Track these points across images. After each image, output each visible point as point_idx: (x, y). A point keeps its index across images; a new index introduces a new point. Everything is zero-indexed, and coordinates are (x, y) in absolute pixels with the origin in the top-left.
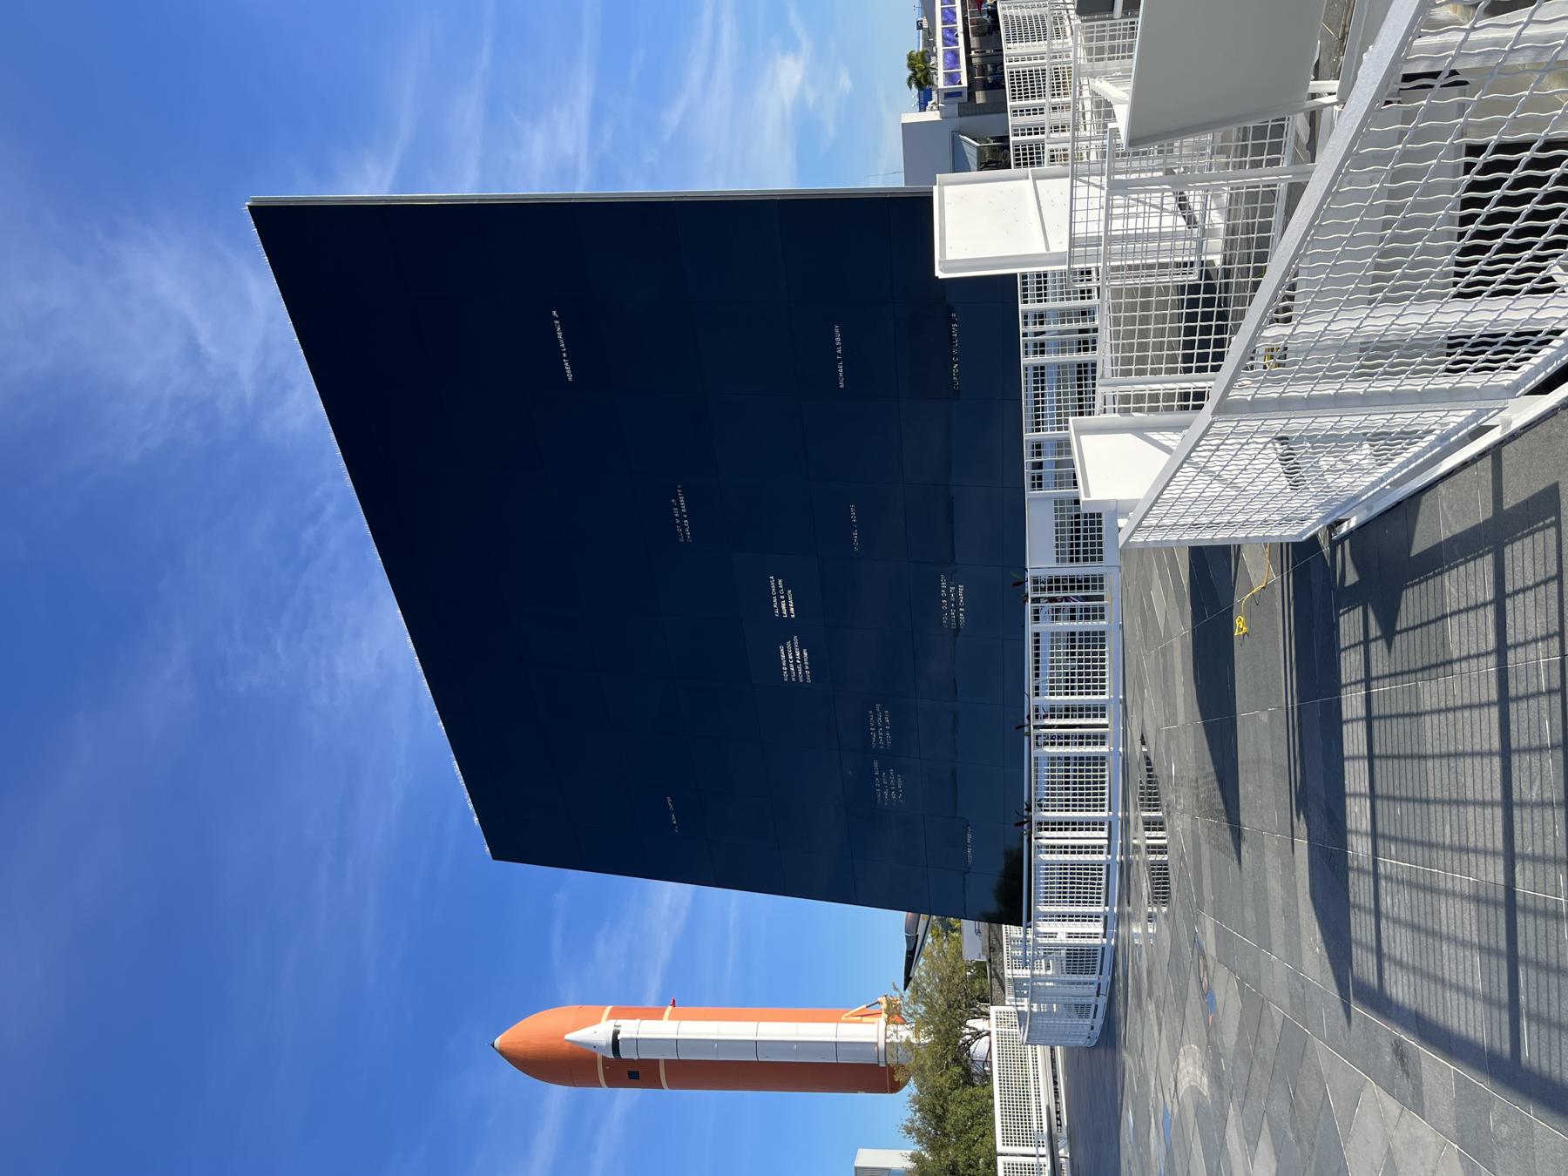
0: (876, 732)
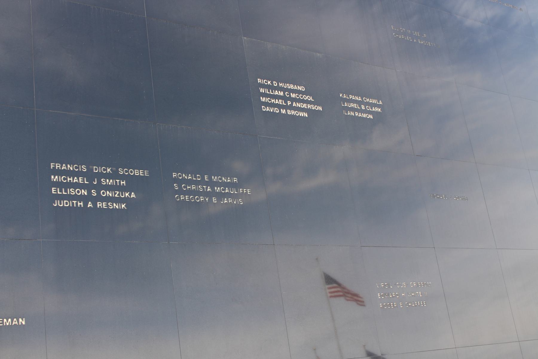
0: (202, 182)
